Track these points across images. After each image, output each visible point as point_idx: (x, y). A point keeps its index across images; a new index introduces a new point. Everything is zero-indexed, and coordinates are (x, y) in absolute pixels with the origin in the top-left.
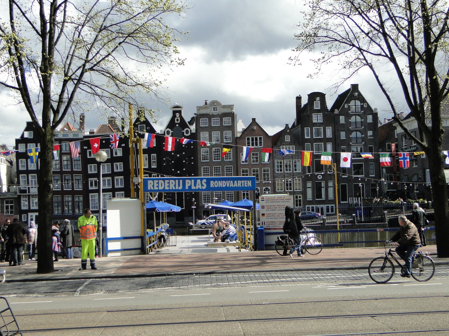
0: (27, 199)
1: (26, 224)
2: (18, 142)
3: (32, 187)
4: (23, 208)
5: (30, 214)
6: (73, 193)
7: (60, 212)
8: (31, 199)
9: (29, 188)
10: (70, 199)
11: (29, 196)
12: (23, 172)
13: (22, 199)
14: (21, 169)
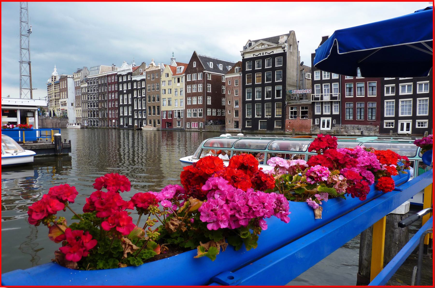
0: (320, 105)
1: (318, 127)
3: (325, 95)
4: (316, 113)
5: (322, 119)
6: (366, 100)
7: (351, 118)
8: (324, 105)
9: (322, 96)
11: (322, 103)
12: (317, 82)
13: (316, 106)
14: (315, 79)
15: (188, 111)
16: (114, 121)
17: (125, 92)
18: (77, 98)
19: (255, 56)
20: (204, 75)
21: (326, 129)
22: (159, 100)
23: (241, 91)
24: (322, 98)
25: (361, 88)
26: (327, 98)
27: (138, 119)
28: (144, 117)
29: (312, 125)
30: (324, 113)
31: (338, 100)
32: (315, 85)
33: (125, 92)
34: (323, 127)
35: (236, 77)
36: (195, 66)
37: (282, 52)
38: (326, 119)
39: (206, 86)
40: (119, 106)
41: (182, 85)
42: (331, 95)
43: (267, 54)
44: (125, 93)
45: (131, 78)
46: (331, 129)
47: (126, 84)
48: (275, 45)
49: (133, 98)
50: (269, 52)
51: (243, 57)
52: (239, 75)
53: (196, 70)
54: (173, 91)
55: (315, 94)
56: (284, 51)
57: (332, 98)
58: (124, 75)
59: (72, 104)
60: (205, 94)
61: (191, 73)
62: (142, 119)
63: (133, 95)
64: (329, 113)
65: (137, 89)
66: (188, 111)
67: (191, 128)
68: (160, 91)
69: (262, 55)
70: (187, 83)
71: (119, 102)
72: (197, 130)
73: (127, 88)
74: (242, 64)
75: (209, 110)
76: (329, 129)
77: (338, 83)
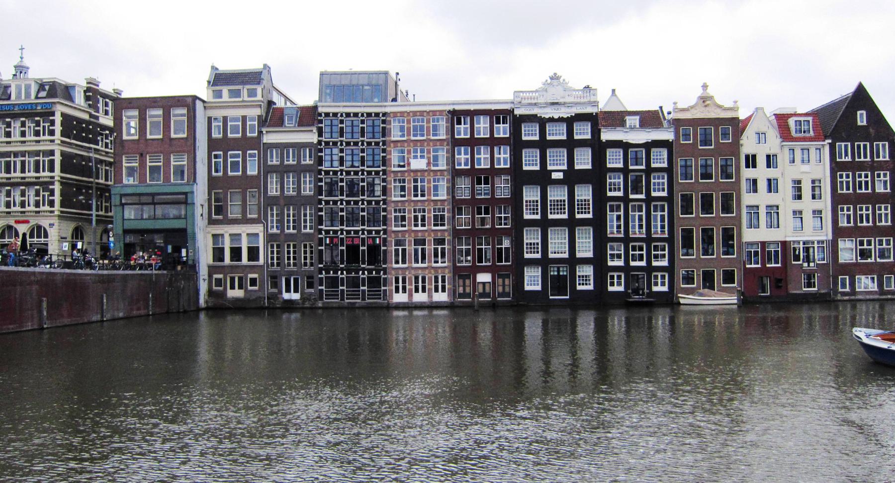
22: (727, 208)
53: (869, 134)
58: (552, 120)
67: (853, 292)
70: (836, 167)
72: (877, 297)
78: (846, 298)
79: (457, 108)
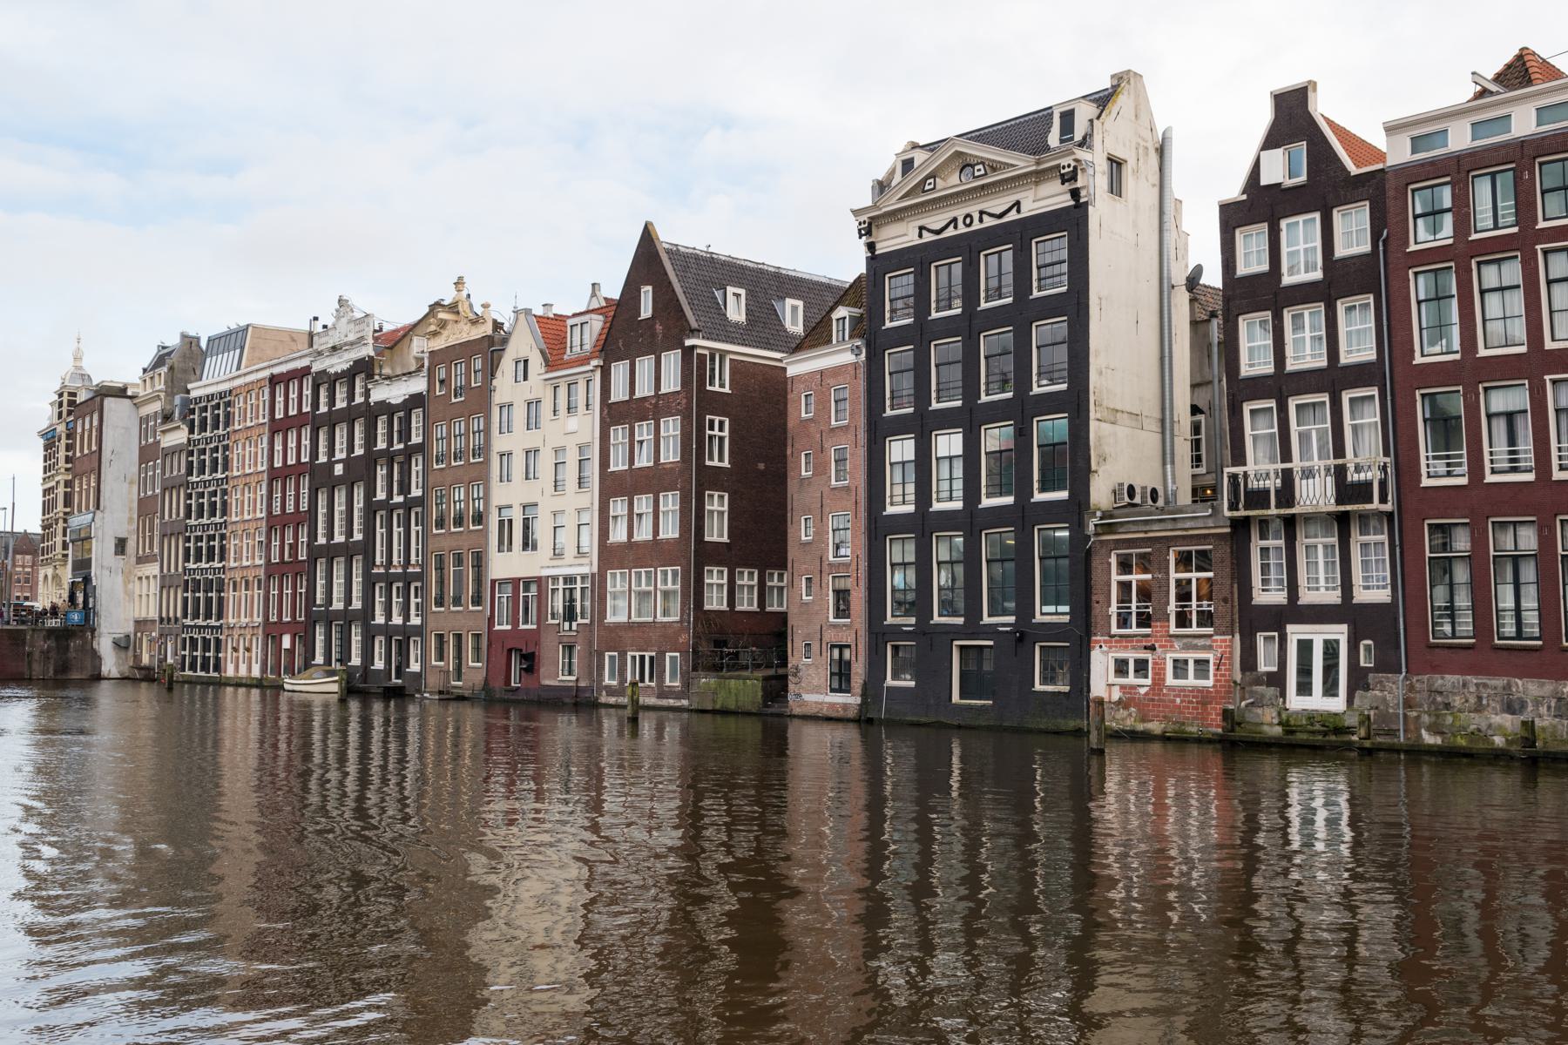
1: (1271, 691)
2: (1232, 217)
4: (1261, 597)
5: (1295, 632)
9: (1287, 476)
10: (1528, 539)
15: (616, 582)
16: (286, 642)
17: (339, 469)
18: (146, 508)
19: (928, 237)
20: (696, 369)
21: (1317, 702)
23: (862, 452)
24: (1287, 494)
25: (1510, 417)
26: (1316, 494)
27: (388, 631)
28: (415, 621)
29: (1238, 677)
30: (1307, 597)
31: (1376, 504)
32: (1247, 408)
33: (339, 469)
34: (1304, 688)
35: (836, 371)
36: (646, 311)
37: (1066, 201)
38: (1319, 635)
39: (701, 430)
40: (315, 553)
41: (584, 426)
42: (1340, 472)
43: (989, 222)
44: (340, 481)
45: (367, 394)
46: (1350, 701)
47: (344, 425)
48: (1023, 163)
49: (371, 509)
50: (998, 204)
51: (871, 247)
52: (847, 358)
54: (545, 463)
55: (1250, 467)
56: (1075, 194)
57: (1349, 491)
59: (121, 545)
60: (696, 480)
61: (631, 354)
62: (407, 633)
63: (370, 492)
64: (1334, 597)
65: (390, 457)
66: (616, 582)
68: (487, 462)
69: (962, 229)
71: (313, 535)
73: (351, 448)
74: (866, 293)
75: (715, 578)
76: (1337, 704)
77: (1375, 391)
78: (612, 700)
79: (276, 371)
